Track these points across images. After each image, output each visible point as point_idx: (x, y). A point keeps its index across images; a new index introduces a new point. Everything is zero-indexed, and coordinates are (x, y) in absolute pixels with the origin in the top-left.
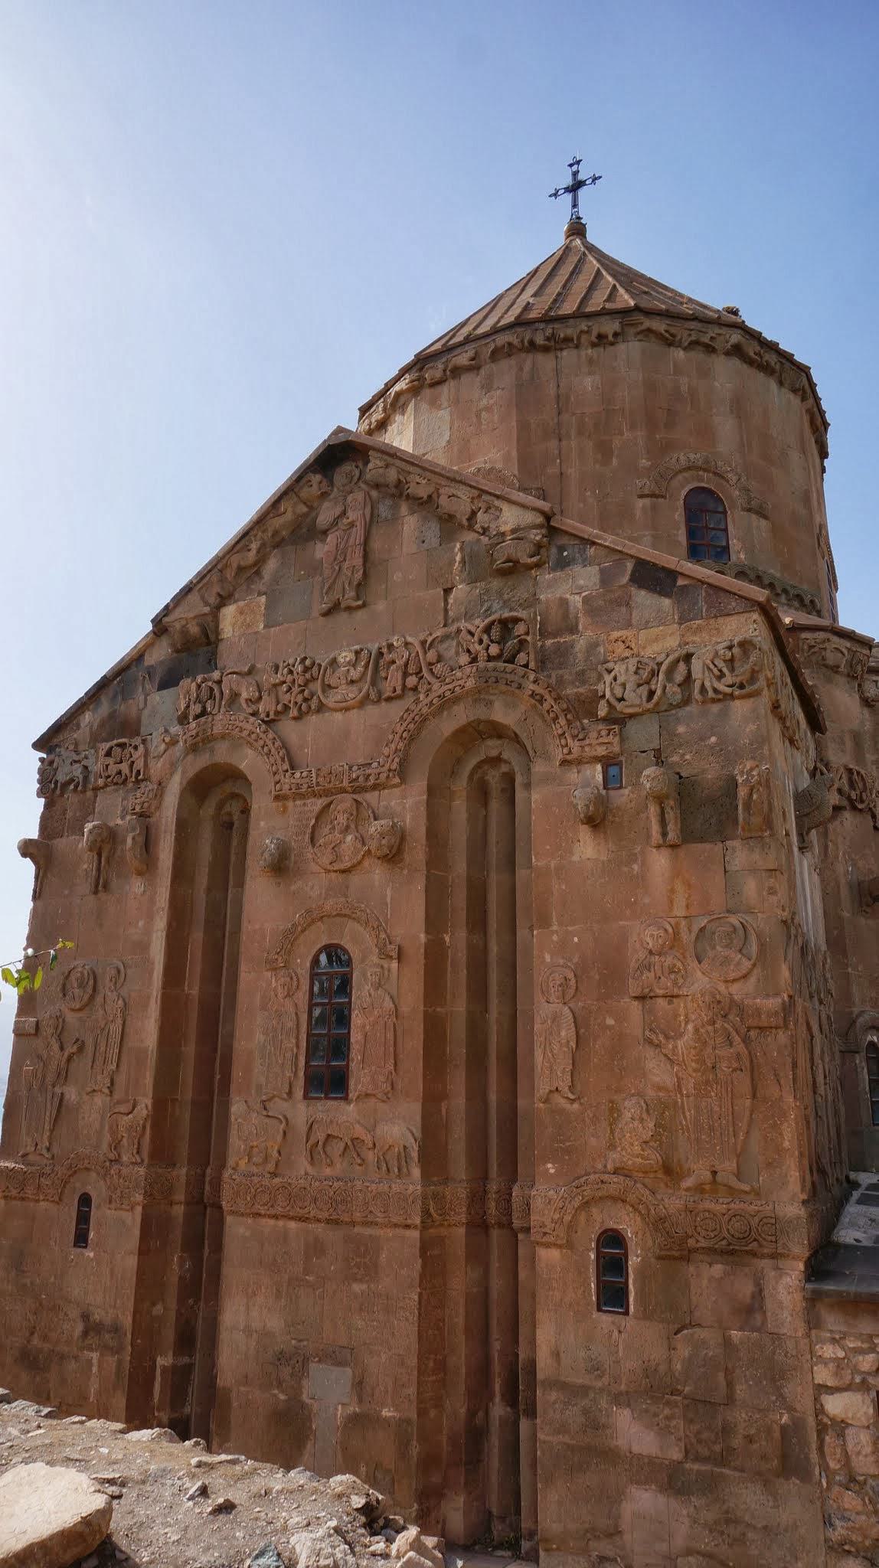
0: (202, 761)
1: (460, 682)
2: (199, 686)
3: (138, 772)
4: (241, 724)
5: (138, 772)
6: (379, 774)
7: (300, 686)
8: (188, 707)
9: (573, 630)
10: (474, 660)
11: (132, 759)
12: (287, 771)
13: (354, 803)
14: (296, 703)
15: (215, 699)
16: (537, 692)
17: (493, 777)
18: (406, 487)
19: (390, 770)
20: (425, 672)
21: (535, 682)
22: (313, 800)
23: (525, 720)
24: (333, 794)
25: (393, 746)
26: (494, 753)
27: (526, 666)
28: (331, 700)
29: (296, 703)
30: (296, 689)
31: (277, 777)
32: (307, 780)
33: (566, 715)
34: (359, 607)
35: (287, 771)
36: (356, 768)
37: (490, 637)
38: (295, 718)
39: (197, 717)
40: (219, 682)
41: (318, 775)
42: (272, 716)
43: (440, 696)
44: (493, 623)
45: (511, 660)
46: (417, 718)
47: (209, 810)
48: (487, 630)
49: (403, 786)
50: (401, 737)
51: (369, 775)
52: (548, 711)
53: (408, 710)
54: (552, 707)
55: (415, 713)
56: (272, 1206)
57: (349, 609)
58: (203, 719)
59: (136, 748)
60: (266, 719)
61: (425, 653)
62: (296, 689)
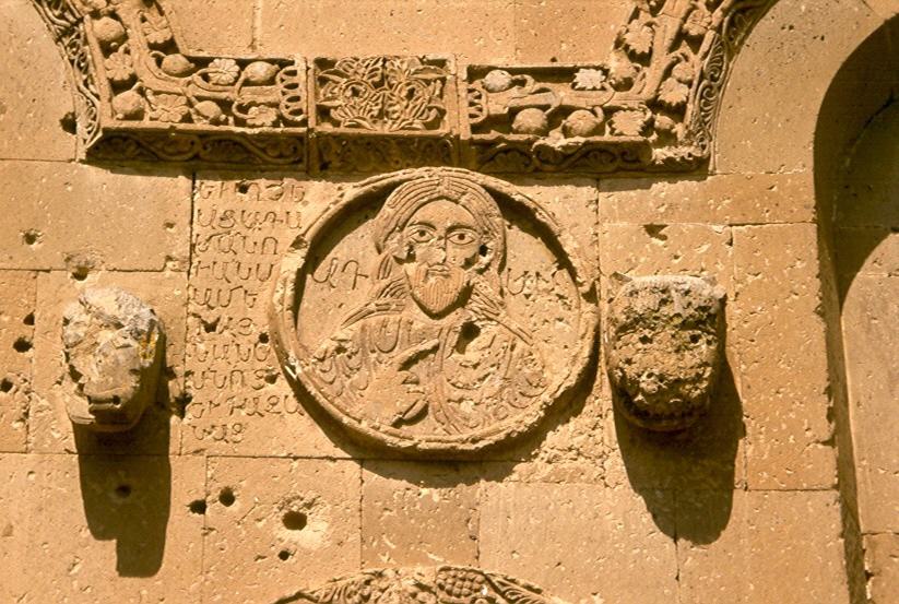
6: (609, 112)
25: (668, 25)
31: (118, 67)
32: (275, 93)
36: (505, 78)
51: (565, 111)
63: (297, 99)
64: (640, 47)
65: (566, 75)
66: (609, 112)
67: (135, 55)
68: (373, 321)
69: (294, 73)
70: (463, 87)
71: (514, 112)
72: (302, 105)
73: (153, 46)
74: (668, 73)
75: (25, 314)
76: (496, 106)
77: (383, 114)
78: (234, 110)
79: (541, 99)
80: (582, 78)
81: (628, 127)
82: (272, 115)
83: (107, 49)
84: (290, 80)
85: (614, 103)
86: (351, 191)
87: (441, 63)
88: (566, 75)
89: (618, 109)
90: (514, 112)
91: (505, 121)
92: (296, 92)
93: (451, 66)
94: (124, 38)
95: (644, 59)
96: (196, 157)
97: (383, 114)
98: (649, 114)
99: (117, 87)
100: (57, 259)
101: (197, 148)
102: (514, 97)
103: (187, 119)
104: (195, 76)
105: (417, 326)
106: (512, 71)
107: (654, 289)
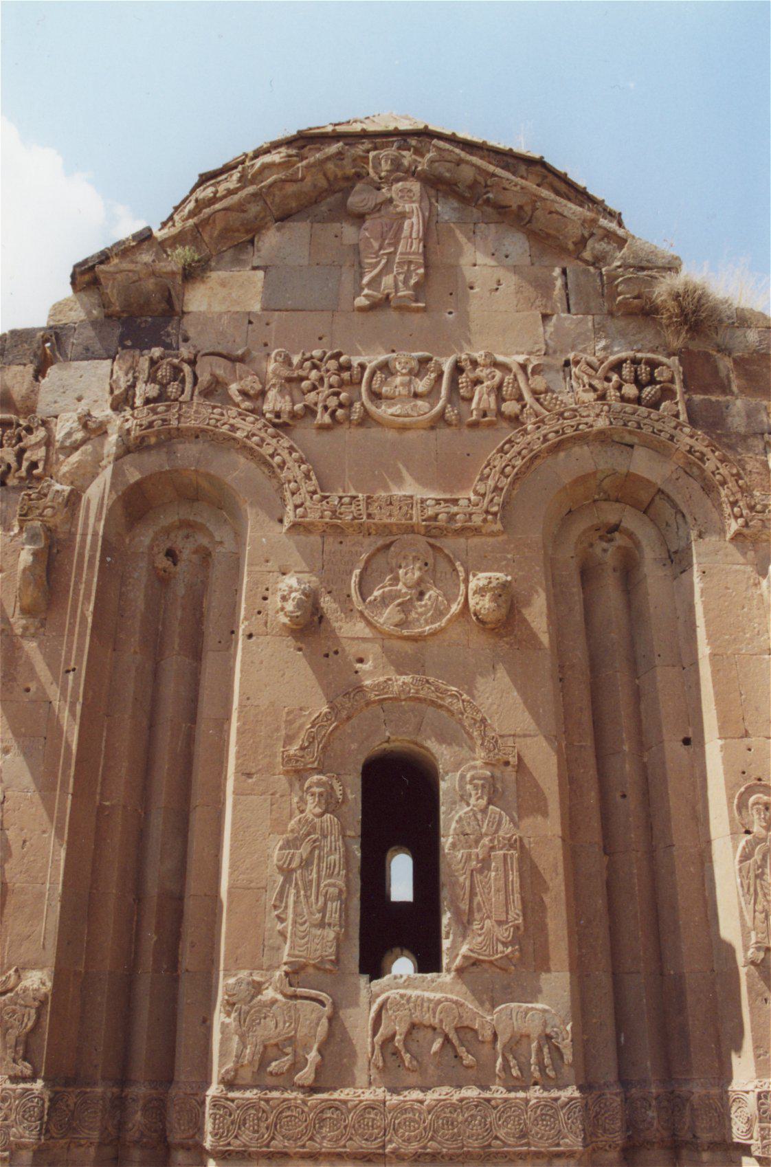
0: (154, 462)
1: (585, 420)
2: (153, 362)
3: (34, 465)
4: (232, 421)
5: (34, 465)
6: (471, 514)
7: (331, 386)
8: (133, 386)
9: (725, 389)
10: (602, 397)
11: (21, 444)
12: (315, 492)
13: (429, 548)
14: (326, 408)
15: (183, 381)
16: (697, 448)
17: (607, 554)
18: (484, 191)
19: (487, 512)
20: (528, 397)
21: (692, 437)
22: (360, 537)
23: (677, 479)
24: (391, 533)
25: (491, 482)
26: (612, 519)
27: (677, 416)
28: (385, 411)
30: (325, 390)
33: (737, 481)
34: (418, 310)
35: (315, 492)
37: (620, 376)
38: (323, 428)
39: (147, 401)
40: (192, 363)
41: (368, 504)
42: (285, 418)
43: (557, 432)
44: (625, 361)
45: (655, 405)
46: (524, 452)
47: (145, 537)
48: (617, 367)
49: (504, 537)
50: (502, 472)
52: (713, 473)
54: (718, 469)
56: (311, 1139)
57: (402, 309)
58: (161, 407)
59: (29, 430)
61: (528, 379)
62: (325, 390)
63: (360, 510)
64: (482, 491)
65: (455, 502)
66: (471, 514)
67: (303, 495)
68: (386, 589)
69: (359, 501)
70: (419, 505)
71: (437, 515)
72: (361, 512)
73: (309, 492)
74: (492, 500)
75: (265, 587)
76: (430, 512)
77: (390, 515)
78: (337, 514)
79: (447, 510)
80: (461, 502)
81: (477, 520)
82: (350, 517)
83: (293, 494)
84: (358, 503)
85: (473, 511)
86: (380, 542)
87: (411, 497)
88: (455, 502)
89: (473, 514)
90: (437, 515)
91: (435, 518)
92: (360, 507)
93: (415, 498)
94: (299, 489)
95: (483, 495)
96: (324, 531)
97: (390, 515)
98: (485, 516)
99: (296, 507)
100: (276, 568)
101: (325, 528)
102: (437, 509)
103: (322, 517)
104: (324, 503)
105: (404, 591)
106: (436, 500)
107: (486, 578)
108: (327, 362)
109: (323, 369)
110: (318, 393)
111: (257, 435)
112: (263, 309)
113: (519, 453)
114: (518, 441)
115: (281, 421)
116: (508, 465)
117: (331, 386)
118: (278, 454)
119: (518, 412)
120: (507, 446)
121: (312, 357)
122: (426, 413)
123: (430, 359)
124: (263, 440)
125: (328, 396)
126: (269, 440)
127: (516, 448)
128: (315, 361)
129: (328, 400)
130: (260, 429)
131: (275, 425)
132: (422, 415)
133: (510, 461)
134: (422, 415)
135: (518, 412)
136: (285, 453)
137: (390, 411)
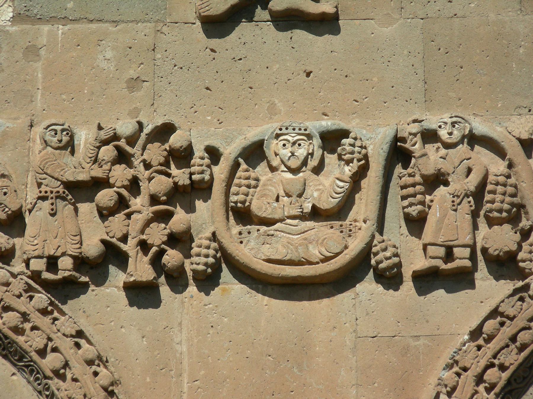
29: (144, 246)
50: (479, 379)
53: (495, 313)
55: (520, 322)
60: (47, 276)
108: (144, 148)
109: (136, 162)
110: (129, 216)
111: (13, 310)
112: (17, 18)
113: (513, 339)
114: (511, 312)
115: (60, 275)
116: (492, 365)
117: (154, 200)
118: (55, 350)
119: (514, 247)
120: (490, 325)
121: (115, 137)
122: (337, 254)
123: (345, 134)
124: (25, 317)
125: (148, 224)
126: (37, 319)
127: (508, 331)
128: (122, 143)
129: (147, 230)
130: (19, 296)
131: (47, 286)
132: (326, 259)
133: (495, 357)
134: (326, 259)
135: (514, 247)
136: (65, 345)
137: (268, 251)
